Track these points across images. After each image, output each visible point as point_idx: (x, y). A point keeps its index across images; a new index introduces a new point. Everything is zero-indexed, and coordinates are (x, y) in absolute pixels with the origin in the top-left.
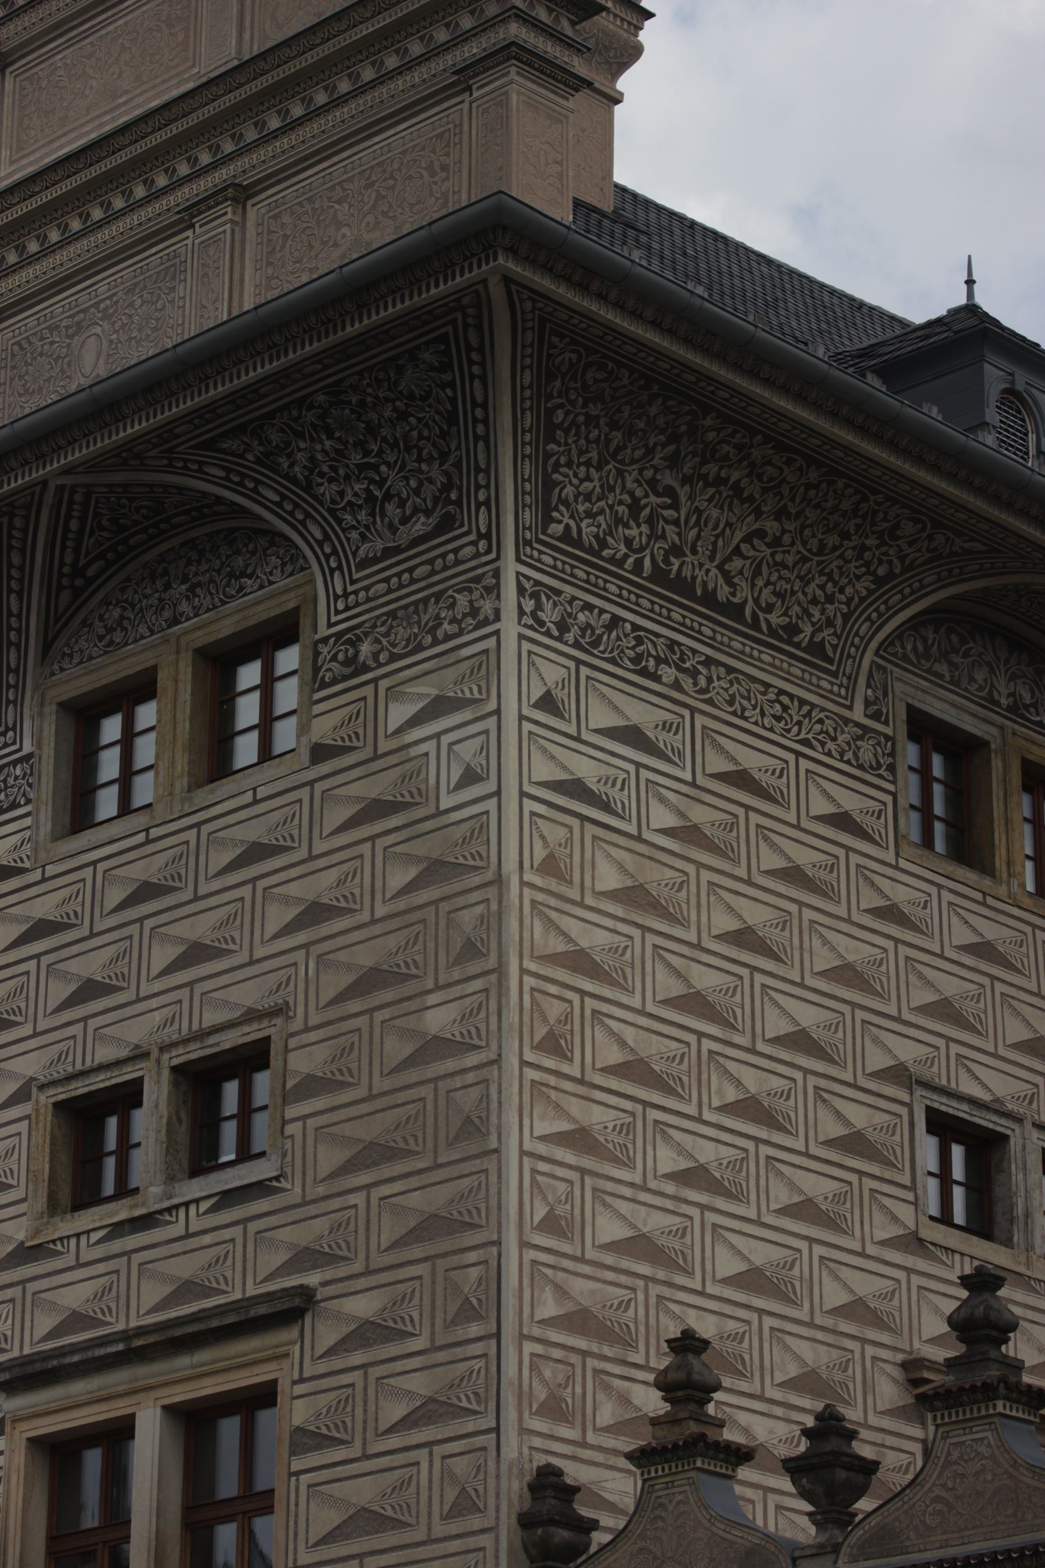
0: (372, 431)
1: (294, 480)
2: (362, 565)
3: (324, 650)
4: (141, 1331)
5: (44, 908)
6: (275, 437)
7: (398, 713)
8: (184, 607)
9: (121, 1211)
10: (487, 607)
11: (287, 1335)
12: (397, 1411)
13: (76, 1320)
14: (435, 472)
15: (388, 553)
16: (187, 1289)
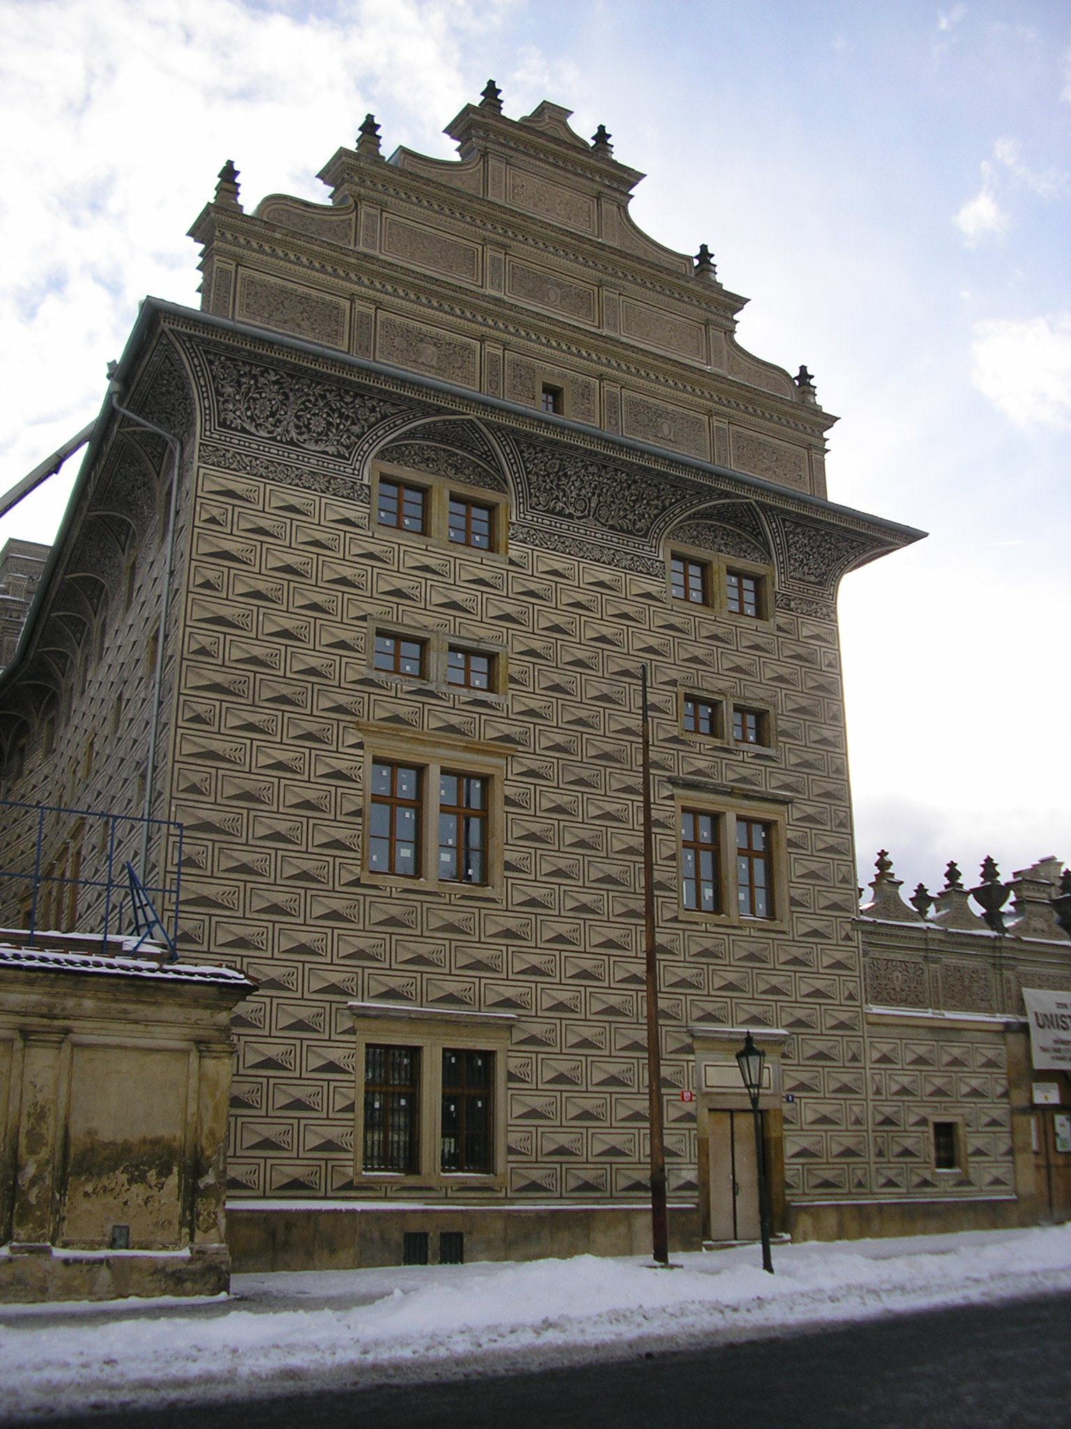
0: (818, 547)
1: (788, 542)
2: (791, 577)
3: (779, 596)
4: (725, 786)
5: (676, 621)
6: (799, 530)
7: (805, 632)
8: (723, 548)
9: (718, 742)
10: (832, 616)
11: (783, 808)
12: (822, 846)
13: (698, 772)
14: (824, 567)
15: (800, 579)
16: (743, 779)
